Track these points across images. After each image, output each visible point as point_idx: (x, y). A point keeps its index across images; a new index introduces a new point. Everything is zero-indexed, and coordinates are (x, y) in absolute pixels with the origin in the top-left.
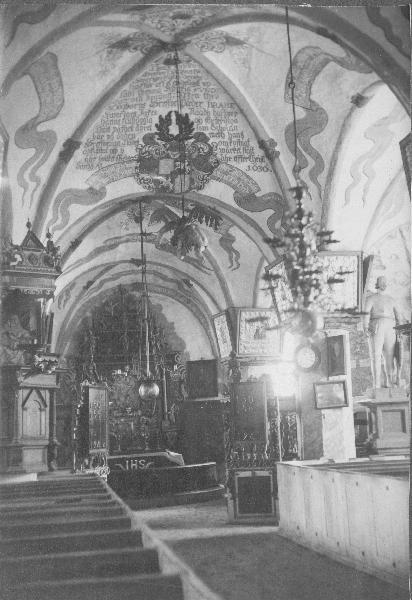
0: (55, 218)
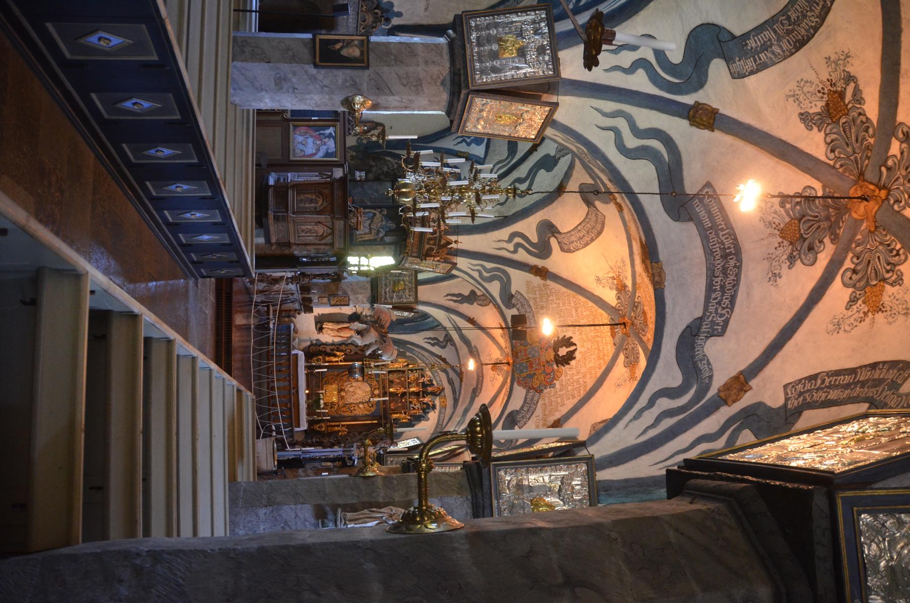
0: (487, 271)
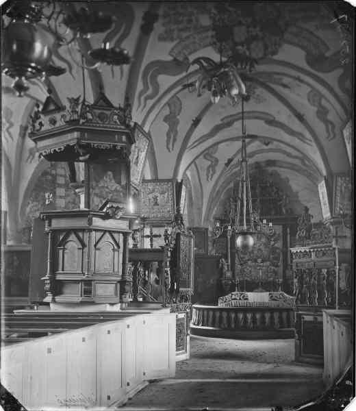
0: (146, 88)
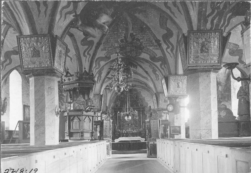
0: (96, 66)
